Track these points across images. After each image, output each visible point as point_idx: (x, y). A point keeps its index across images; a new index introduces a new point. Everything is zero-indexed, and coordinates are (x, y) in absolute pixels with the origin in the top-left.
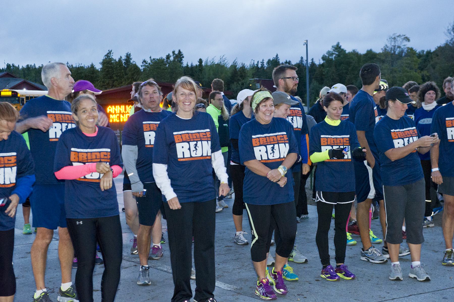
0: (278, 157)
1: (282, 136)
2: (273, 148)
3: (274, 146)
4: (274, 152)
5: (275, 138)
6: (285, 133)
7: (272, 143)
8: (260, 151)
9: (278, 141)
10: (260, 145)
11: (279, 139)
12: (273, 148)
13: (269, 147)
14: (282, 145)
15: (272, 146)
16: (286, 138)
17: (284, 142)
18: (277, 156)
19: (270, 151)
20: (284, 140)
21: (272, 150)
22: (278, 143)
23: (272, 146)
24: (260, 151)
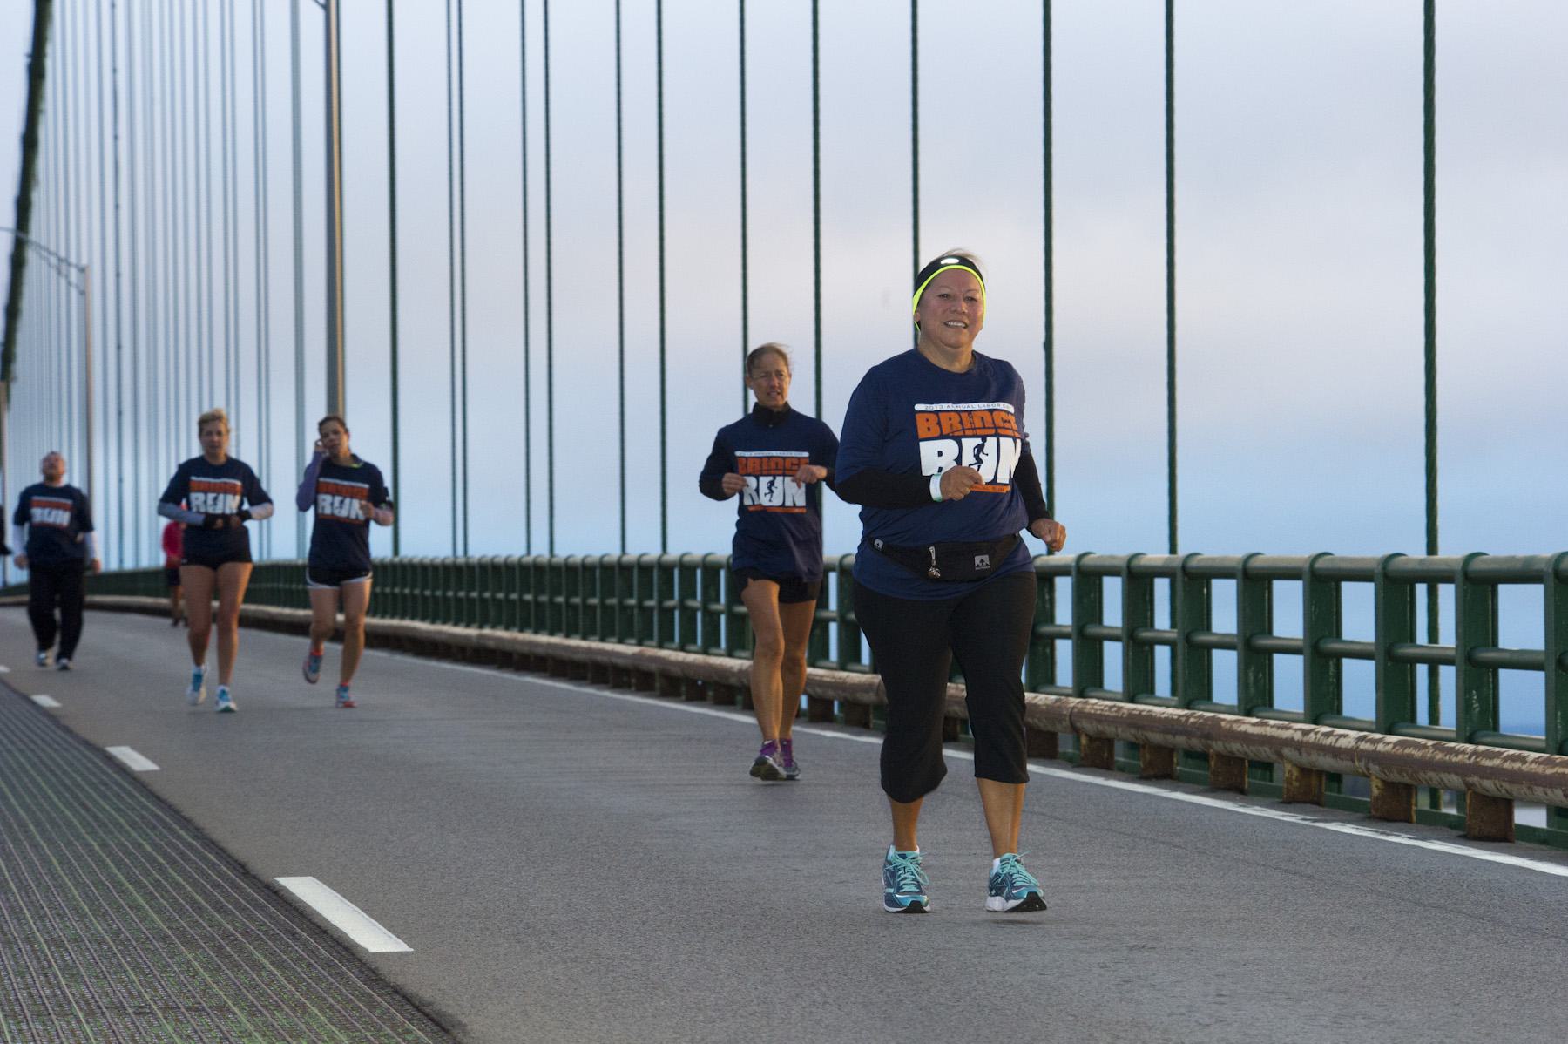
2: (980, 448)
3: (984, 440)
4: (979, 461)
5: (987, 416)
7: (979, 432)
8: (940, 454)
9: (996, 428)
10: (942, 437)
12: (980, 448)
15: (979, 441)
21: (977, 456)
22: (998, 436)
23: (979, 441)
24: (940, 454)
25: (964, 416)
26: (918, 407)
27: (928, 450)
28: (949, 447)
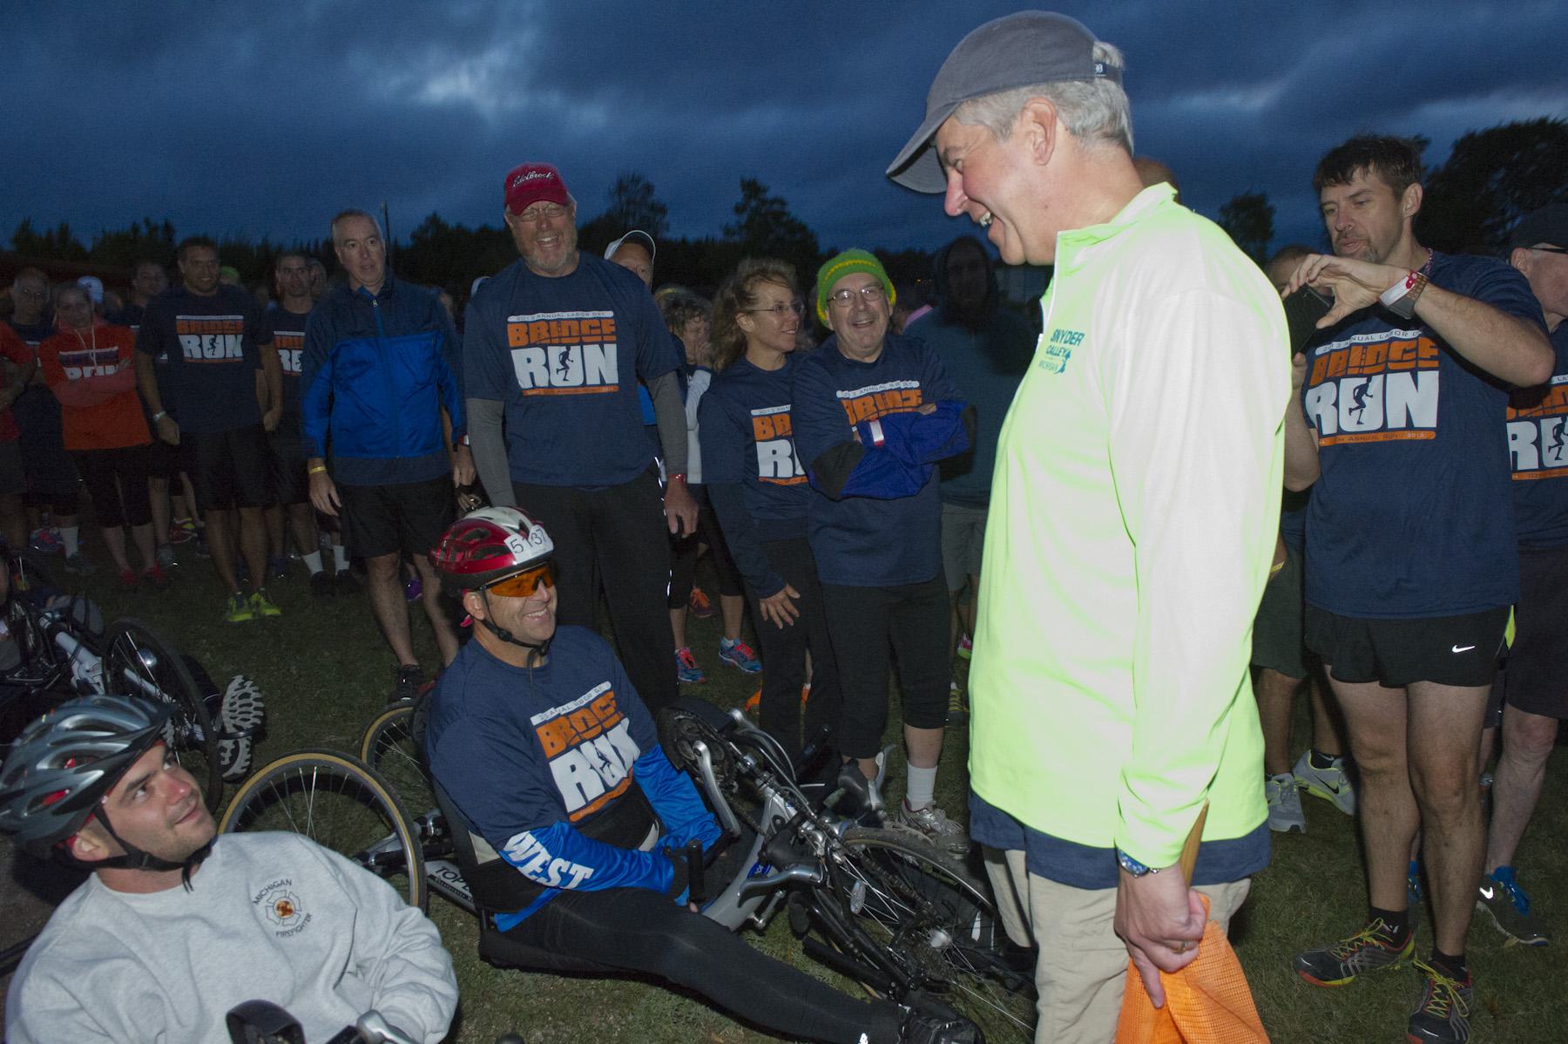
0: (580, 382)
1: (597, 323)
2: (565, 356)
4: (566, 368)
6: (610, 314)
7: (564, 341)
8: (529, 361)
9: (581, 336)
10: (530, 345)
11: (585, 330)
12: (565, 356)
13: (555, 352)
14: (592, 351)
15: (564, 349)
16: (608, 328)
17: (599, 339)
18: (575, 379)
19: (555, 363)
20: (602, 335)
21: (563, 362)
22: (581, 344)
23: (564, 349)
24: (529, 361)
25: (553, 325)
26: (512, 319)
27: (518, 356)
28: (536, 353)
